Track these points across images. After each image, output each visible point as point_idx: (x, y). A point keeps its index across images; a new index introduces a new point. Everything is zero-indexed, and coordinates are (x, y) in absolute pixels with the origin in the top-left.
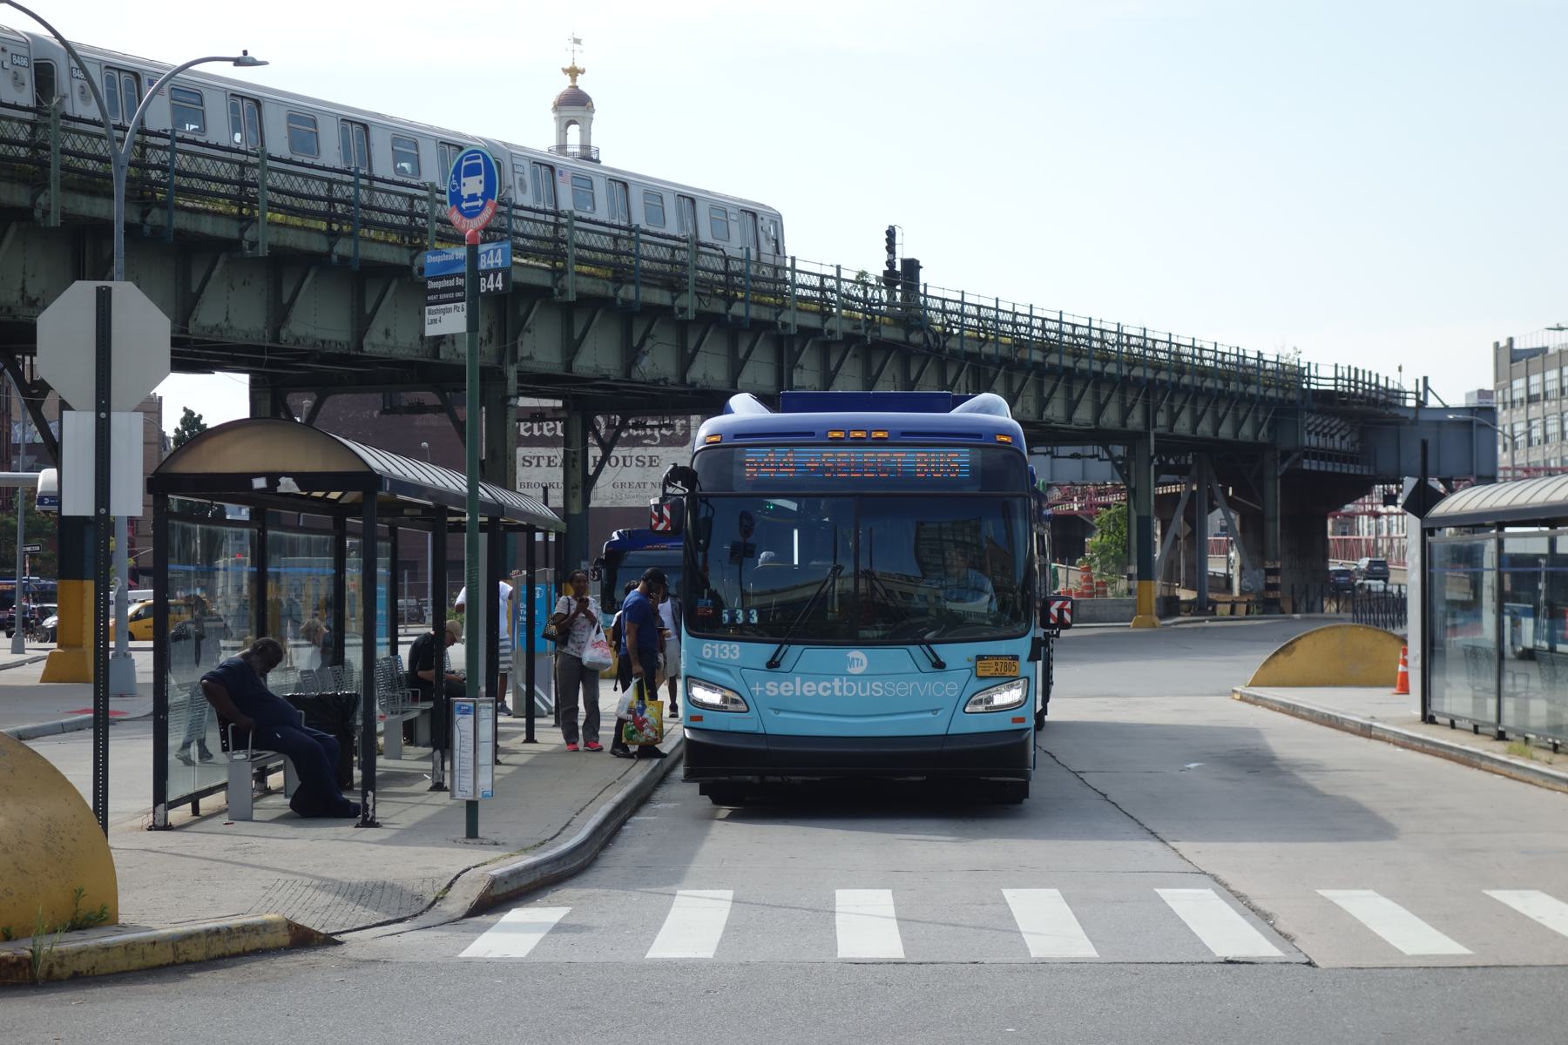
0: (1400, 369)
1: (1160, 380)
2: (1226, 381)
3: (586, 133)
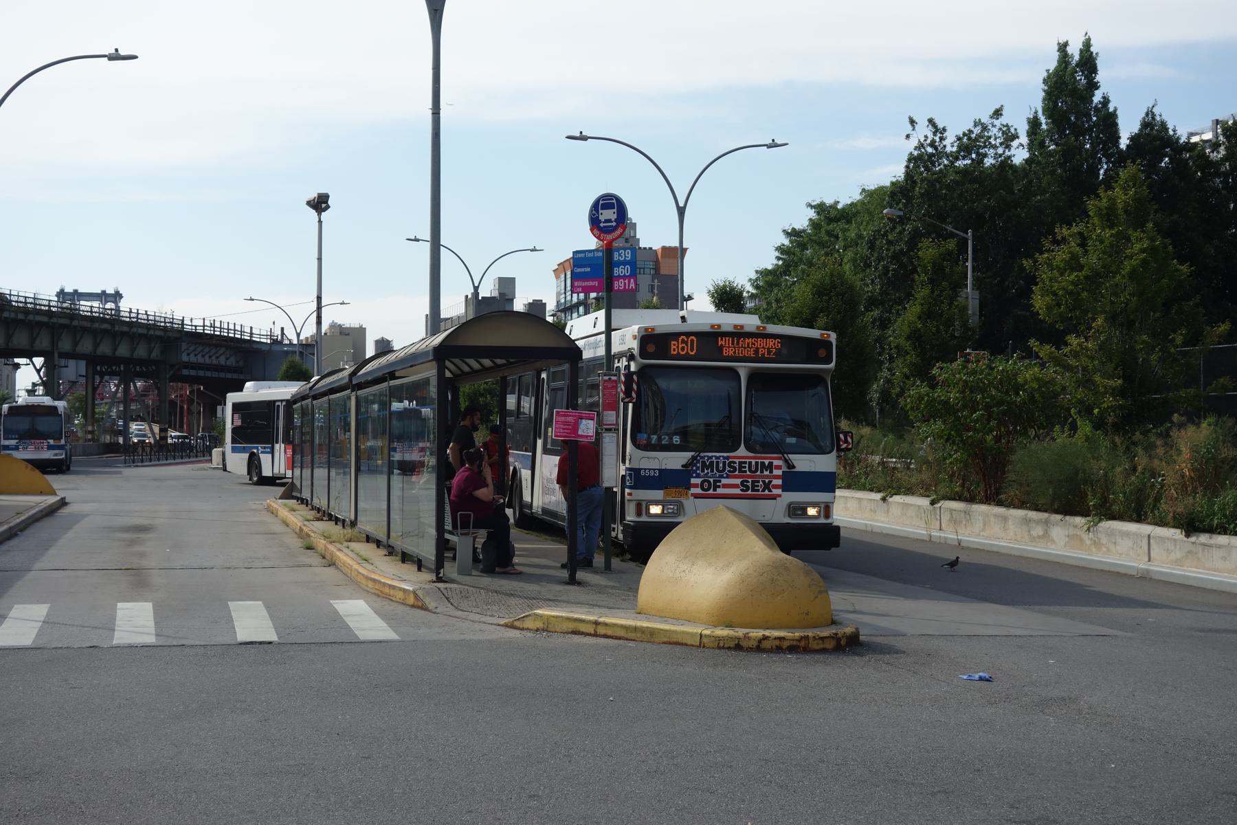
0: (274, 323)
1: (53, 323)
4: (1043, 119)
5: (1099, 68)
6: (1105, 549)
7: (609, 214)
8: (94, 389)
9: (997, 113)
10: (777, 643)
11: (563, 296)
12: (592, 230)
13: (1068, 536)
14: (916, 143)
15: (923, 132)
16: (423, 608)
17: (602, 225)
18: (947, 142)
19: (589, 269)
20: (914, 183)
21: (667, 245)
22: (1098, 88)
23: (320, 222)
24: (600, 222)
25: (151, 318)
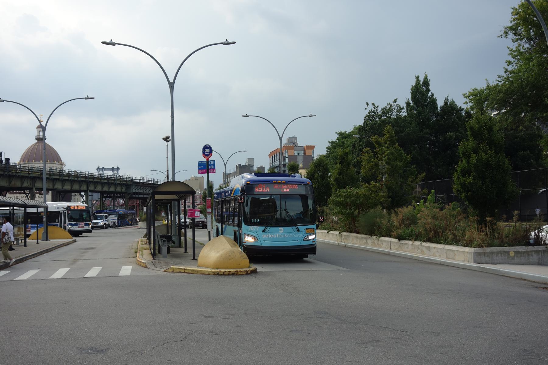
2: (108, 181)
3: (44, 133)
4: (411, 102)
5: (430, 84)
6: (380, 246)
7: (207, 151)
8: (103, 202)
9: (395, 101)
10: (229, 273)
11: (272, 164)
12: (203, 155)
13: (372, 242)
14: (368, 111)
15: (371, 107)
16: (147, 267)
17: (206, 154)
18: (378, 111)
19: (202, 167)
20: (367, 125)
21: (308, 145)
22: (430, 91)
23: (167, 145)
24: (205, 153)
25: (121, 177)
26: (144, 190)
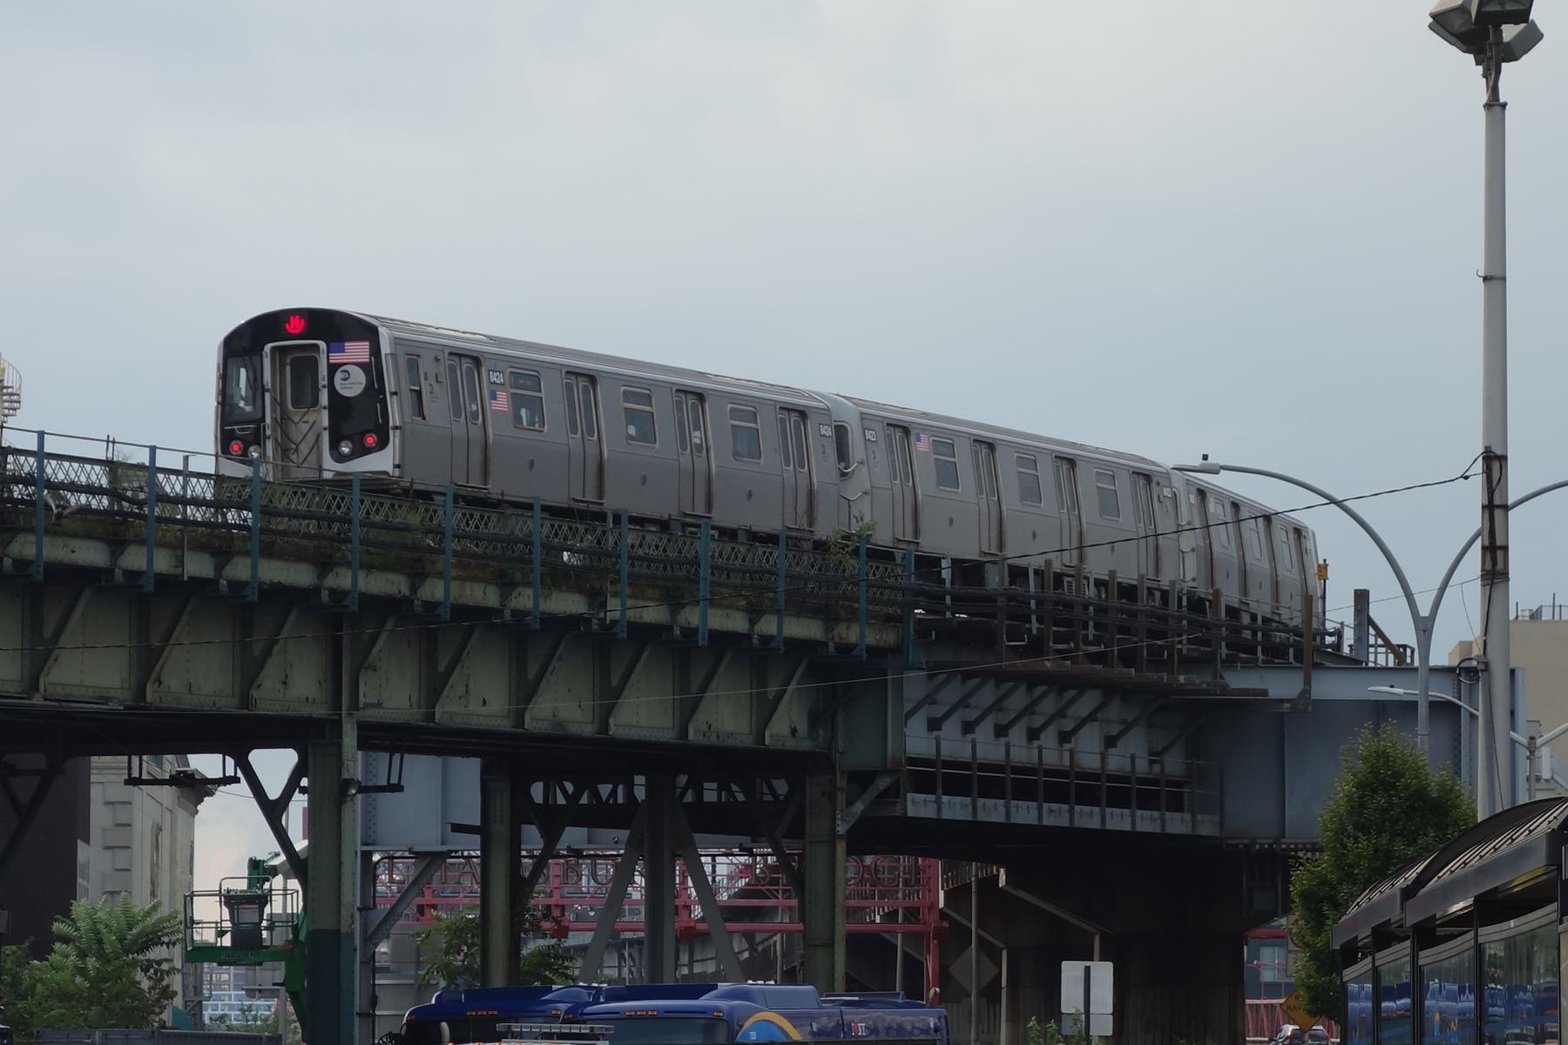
1: (230, 582)
8: (520, 888)
26: (1049, 738)
